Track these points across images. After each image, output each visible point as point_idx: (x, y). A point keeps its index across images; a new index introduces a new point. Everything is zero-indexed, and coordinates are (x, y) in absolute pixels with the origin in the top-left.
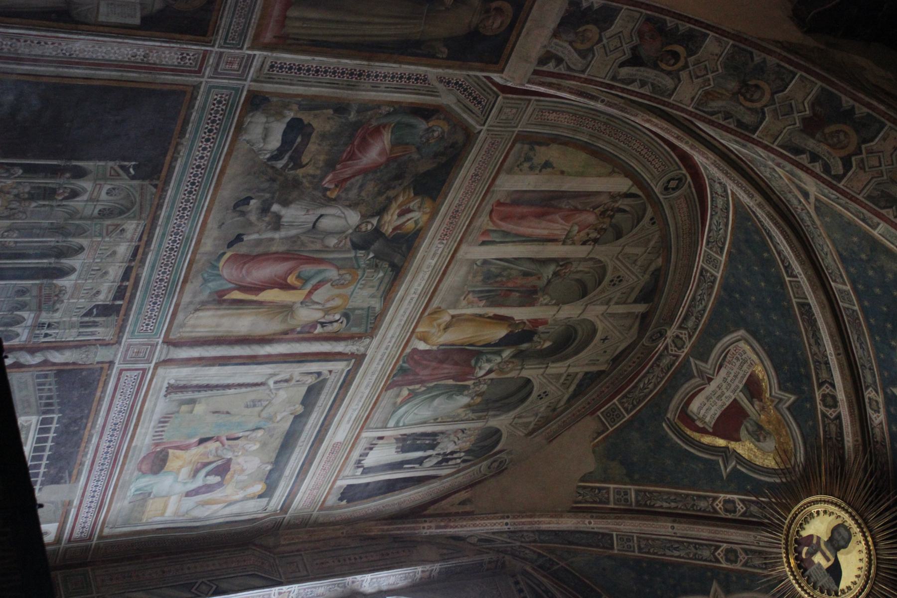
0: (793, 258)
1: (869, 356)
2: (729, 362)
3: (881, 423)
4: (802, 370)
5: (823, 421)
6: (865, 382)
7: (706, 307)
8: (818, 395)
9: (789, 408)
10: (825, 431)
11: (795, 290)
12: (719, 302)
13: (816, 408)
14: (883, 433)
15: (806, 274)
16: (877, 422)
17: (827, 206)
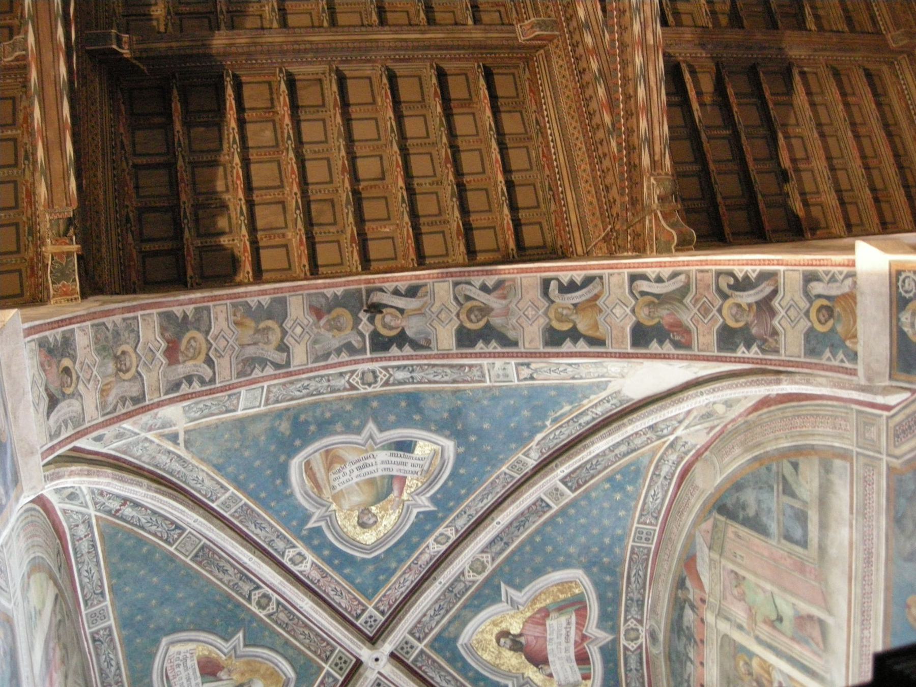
0: (186, 510)
1: (272, 526)
2: (174, 677)
3: (313, 563)
4: (230, 606)
5: (272, 620)
6: (278, 553)
7: (118, 664)
8: (254, 608)
9: (246, 645)
10: (280, 626)
11: (183, 550)
12: (127, 642)
13: (262, 620)
14: (320, 568)
15: (200, 515)
16: (309, 565)
17: (195, 430)
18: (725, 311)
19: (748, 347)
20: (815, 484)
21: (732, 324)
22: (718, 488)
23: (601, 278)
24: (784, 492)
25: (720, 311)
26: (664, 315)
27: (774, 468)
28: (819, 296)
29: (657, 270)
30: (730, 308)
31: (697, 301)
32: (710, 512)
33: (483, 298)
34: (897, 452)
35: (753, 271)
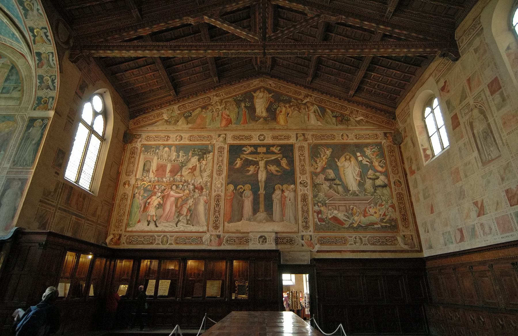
18: (47, 77)
19: (39, 83)
20: (15, 96)
21: (44, 79)
22: (18, 66)
23: (51, 44)
24: (14, 87)
25: (47, 76)
26: (45, 61)
27: (20, 85)
28: (49, 100)
29: (55, 60)
30: (48, 78)
31: (49, 70)
32: (12, 64)
33: (35, 9)
34: (18, 117)
35: (56, 84)
